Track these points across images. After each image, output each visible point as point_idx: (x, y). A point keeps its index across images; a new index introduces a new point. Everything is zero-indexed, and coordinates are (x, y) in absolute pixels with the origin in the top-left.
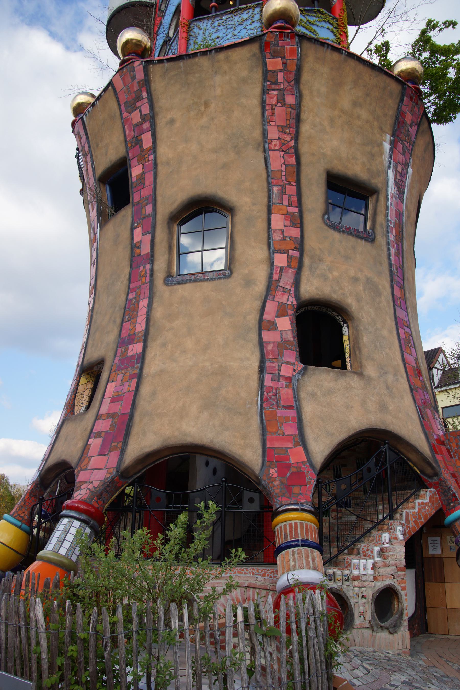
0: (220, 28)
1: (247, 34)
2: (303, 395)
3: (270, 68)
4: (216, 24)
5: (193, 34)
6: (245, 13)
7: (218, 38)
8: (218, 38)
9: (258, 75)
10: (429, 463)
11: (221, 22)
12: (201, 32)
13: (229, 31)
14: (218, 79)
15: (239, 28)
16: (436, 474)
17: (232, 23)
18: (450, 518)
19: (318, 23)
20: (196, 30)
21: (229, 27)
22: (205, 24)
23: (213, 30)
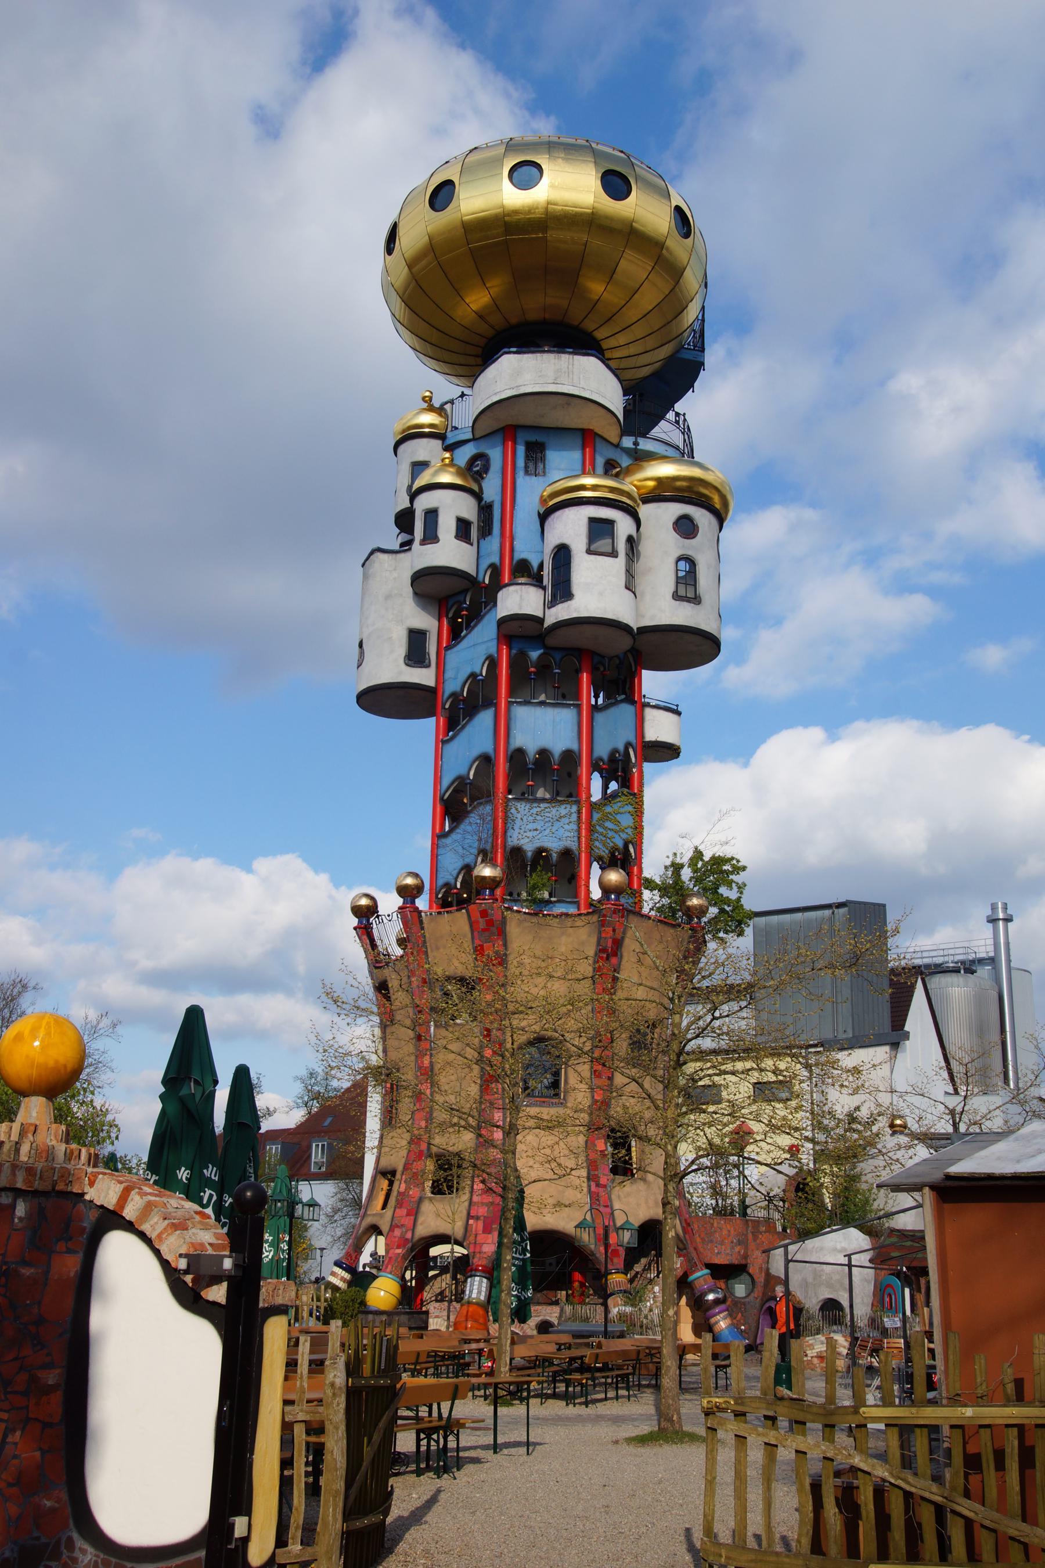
0: (538, 818)
1: (565, 835)
2: (613, 1197)
3: (603, 935)
4: (534, 811)
5: (510, 815)
6: (563, 807)
7: (536, 830)
8: (536, 830)
9: (594, 940)
10: (681, 1241)
11: (539, 809)
12: (519, 816)
13: (547, 824)
14: (564, 939)
15: (557, 825)
16: (685, 1249)
17: (550, 815)
18: (691, 1278)
19: (622, 810)
20: (513, 811)
21: (547, 819)
22: (523, 806)
23: (531, 818)
